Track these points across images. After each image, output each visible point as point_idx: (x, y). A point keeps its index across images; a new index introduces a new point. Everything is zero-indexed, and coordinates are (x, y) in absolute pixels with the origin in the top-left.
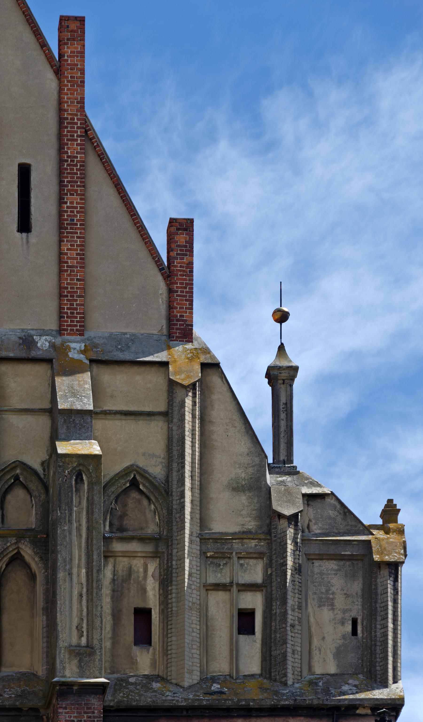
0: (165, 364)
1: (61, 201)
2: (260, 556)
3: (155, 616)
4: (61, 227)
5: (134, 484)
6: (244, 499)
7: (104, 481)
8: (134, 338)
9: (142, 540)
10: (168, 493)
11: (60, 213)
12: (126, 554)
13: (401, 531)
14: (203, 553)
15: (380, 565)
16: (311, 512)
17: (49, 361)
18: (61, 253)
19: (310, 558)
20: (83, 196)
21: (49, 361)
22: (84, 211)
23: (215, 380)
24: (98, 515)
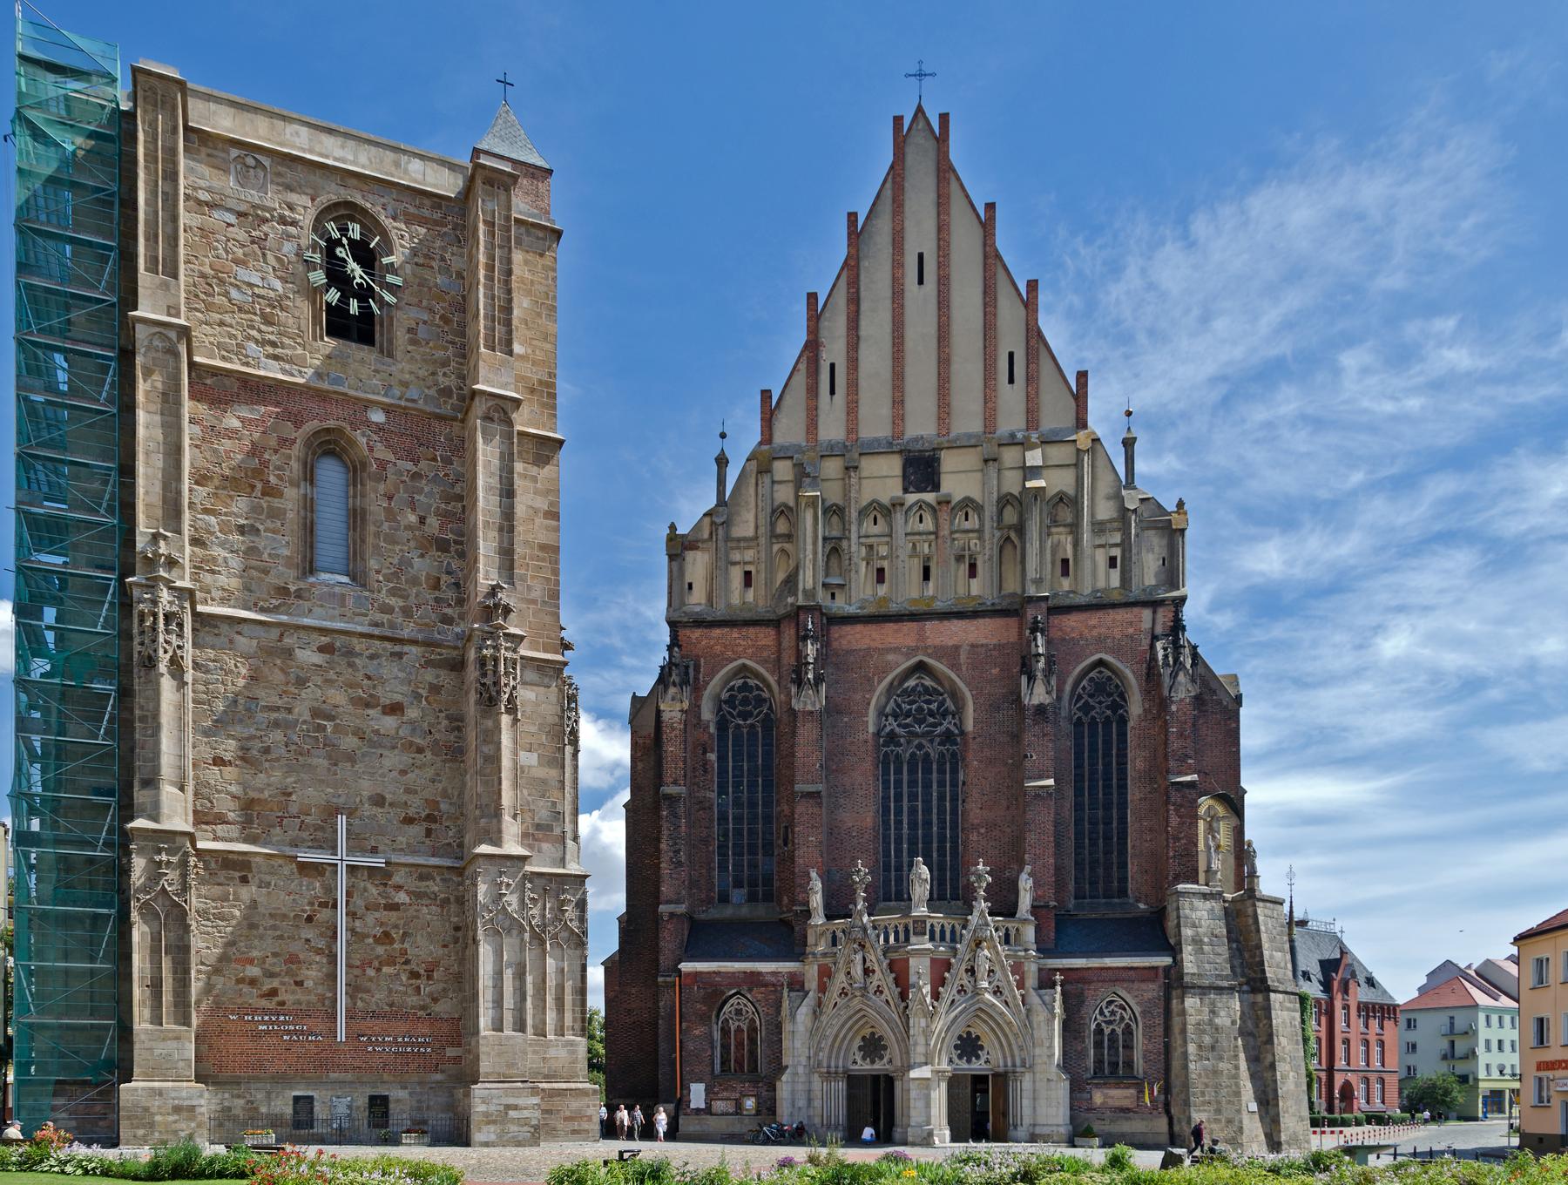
0: (1075, 441)
1: (1028, 367)
4: (1028, 380)
5: (1061, 499)
6: (1112, 503)
7: (1047, 498)
8: (1061, 429)
9: (1065, 526)
10: (1077, 502)
11: (1027, 373)
12: (1058, 533)
13: (1186, 513)
14: (1093, 531)
16: (1143, 507)
17: (1022, 444)
18: (1027, 392)
19: (1143, 529)
20: (1038, 364)
21: (1022, 444)
22: (1038, 371)
23: (1098, 446)
24: (1045, 515)
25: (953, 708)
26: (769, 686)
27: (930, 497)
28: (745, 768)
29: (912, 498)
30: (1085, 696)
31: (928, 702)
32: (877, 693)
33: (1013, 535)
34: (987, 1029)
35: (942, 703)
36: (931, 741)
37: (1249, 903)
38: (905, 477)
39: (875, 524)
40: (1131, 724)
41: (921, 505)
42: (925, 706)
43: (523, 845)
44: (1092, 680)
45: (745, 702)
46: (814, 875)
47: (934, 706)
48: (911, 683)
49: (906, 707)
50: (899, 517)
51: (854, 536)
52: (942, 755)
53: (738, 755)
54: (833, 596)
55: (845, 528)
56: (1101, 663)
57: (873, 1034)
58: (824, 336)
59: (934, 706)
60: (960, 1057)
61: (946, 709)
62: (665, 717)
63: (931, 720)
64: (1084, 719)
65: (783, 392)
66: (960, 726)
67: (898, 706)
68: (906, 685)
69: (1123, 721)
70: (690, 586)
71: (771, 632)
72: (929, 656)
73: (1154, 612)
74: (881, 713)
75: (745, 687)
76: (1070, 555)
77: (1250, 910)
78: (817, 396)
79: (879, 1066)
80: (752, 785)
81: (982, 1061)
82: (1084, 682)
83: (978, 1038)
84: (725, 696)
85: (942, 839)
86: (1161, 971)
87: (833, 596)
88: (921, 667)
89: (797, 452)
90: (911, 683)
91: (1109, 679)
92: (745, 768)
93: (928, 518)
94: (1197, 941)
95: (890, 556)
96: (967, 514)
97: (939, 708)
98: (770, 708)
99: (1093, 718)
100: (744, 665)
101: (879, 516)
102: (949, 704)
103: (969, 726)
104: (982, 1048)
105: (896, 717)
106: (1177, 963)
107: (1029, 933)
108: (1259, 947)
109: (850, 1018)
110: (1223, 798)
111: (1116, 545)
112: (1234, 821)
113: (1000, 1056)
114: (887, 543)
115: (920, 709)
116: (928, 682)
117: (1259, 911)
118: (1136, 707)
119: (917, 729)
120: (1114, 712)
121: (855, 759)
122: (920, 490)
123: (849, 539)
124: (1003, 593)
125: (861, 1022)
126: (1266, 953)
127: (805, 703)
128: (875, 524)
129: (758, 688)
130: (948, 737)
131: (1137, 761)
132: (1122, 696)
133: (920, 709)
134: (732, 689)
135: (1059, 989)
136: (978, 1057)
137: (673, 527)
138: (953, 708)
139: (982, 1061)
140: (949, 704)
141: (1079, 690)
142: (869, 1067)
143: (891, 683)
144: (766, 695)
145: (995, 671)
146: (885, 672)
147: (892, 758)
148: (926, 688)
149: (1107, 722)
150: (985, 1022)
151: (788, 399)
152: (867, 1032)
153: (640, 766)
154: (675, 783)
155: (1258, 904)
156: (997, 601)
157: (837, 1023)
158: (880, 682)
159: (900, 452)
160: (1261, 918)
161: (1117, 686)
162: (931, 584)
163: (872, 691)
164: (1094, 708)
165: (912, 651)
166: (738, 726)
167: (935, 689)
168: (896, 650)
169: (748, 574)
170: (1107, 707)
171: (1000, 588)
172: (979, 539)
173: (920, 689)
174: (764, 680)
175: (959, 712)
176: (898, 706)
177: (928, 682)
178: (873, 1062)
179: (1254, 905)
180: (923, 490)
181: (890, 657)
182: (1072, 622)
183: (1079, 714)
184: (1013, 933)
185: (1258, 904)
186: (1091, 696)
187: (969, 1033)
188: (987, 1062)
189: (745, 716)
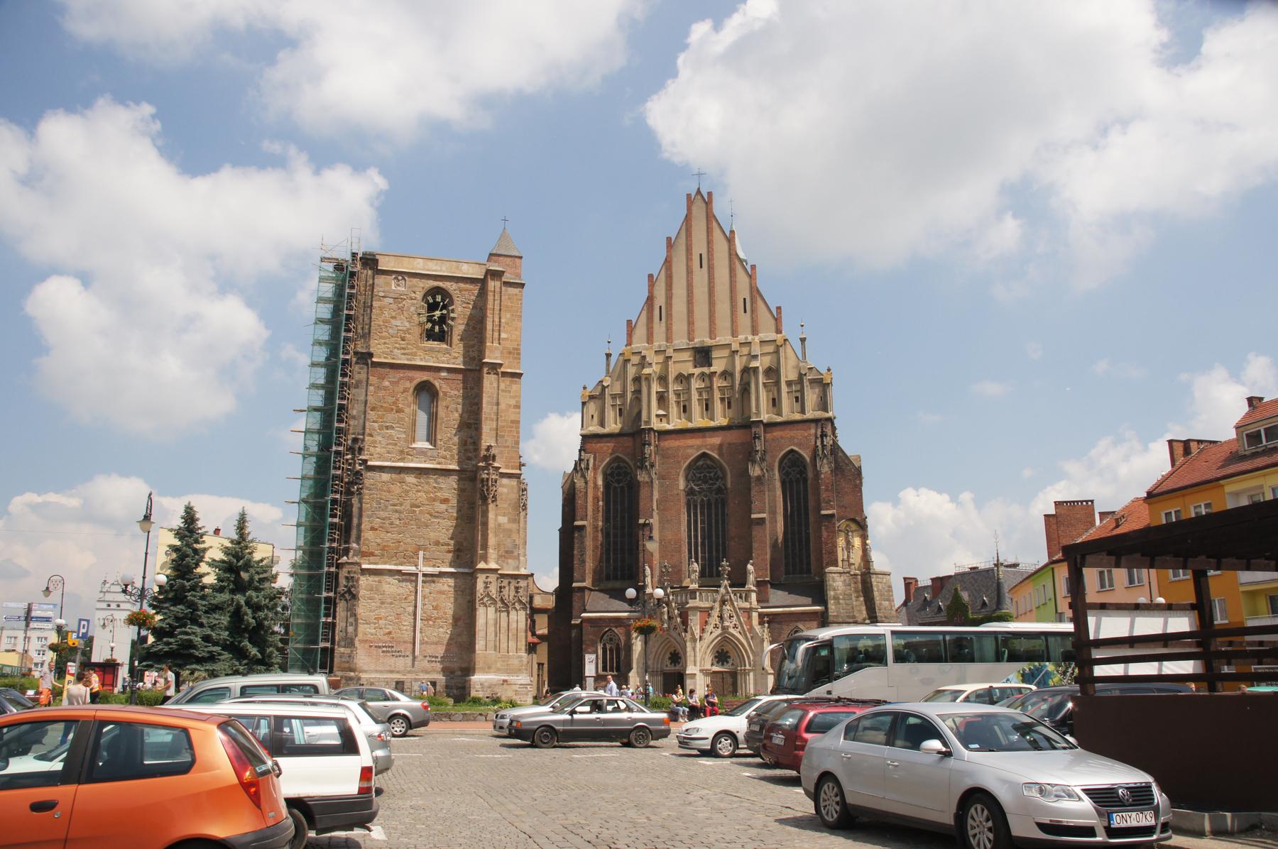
2: (799, 383)
3: (777, 400)
15: (825, 384)
25: (721, 475)
26: (630, 466)
27: (706, 370)
28: (619, 509)
29: (697, 371)
30: (787, 468)
31: (709, 472)
32: (683, 468)
33: (747, 386)
34: (731, 647)
35: (716, 474)
36: (711, 493)
37: (868, 576)
38: (695, 359)
39: (682, 383)
40: (809, 482)
41: (703, 374)
42: (708, 475)
43: (497, 564)
44: (789, 459)
45: (619, 474)
46: (647, 567)
47: (712, 475)
48: (701, 463)
49: (698, 475)
50: (693, 381)
51: (670, 390)
52: (717, 500)
53: (615, 502)
54: (661, 420)
55: (667, 387)
56: (792, 451)
57: (675, 651)
58: (656, 293)
59: (712, 475)
60: (718, 662)
61: (718, 476)
62: (578, 485)
63: (711, 482)
64: (787, 480)
65: (637, 321)
66: (724, 485)
67: (694, 475)
68: (698, 464)
69: (805, 480)
70: (592, 416)
71: (630, 439)
72: (708, 449)
73: (817, 425)
74: (687, 479)
75: (618, 467)
76: (776, 397)
77: (869, 580)
78: (652, 322)
79: (678, 667)
80: (623, 518)
81: (730, 664)
82: (786, 461)
83: (727, 652)
84: (608, 472)
85: (717, 545)
86: (819, 614)
87: (661, 420)
88: (704, 455)
89: (644, 350)
90: (701, 463)
91: (798, 458)
92: (619, 509)
93: (707, 380)
94: (836, 598)
95: (689, 399)
96: (725, 377)
97: (715, 476)
98: (631, 477)
99: (791, 479)
100: (618, 458)
101: (683, 379)
102: (719, 473)
103: (729, 485)
104: (729, 657)
105: (693, 481)
106: (827, 609)
107: (754, 596)
108: (873, 599)
109: (663, 642)
110: (853, 520)
111: (798, 391)
112: (861, 532)
113: (738, 661)
114: (687, 393)
115: (705, 476)
116: (709, 462)
117: (873, 580)
118: (810, 475)
119: (704, 486)
120: (801, 476)
121: (672, 503)
122: (702, 366)
123: (668, 391)
124: (744, 416)
125: (668, 645)
126: (877, 602)
127: (644, 477)
128: (682, 383)
129: (626, 468)
130: (719, 491)
131: (811, 504)
132: (805, 467)
133: (705, 476)
134: (612, 468)
135: (766, 625)
136: (727, 662)
137: (585, 388)
138: (721, 475)
139: (730, 664)
140: (719, 473)
141: (784, 464)
142: (673, 668)
143: (690, 463)
144: (629, 471)
145: (741, 457)
146: (687, 458)
147: (692, 502)
148: (708, 465)
149: (798, 481)
150: (730, 644)
151: (639, 322)
152: (672, 650)
153: (567, 509)
154: (582, 520)
155: (872, 576)
156: (740, 421)
157: (657, 646)
158: (685, 462)
159: (693, 348)
160: (874, 584)
161: (802, 462)
162: (709, 411)
163: (681, 468)
164: (791, 473)
165: (699, 448)
166: (615, 487)
167: (712, 466)
168: (691, 447)
169: (620, 410)
170: (798, 473)
171: (743, 414)
172: (731, 389)
173: (705, 466)
174: (627, 463)
175: (724, 478)
176: (694, 475)
177: (709, 462)
178: (675, 666)
179: (870, 577)
180: (704, 366)
181: (689, 451)
182: (777, 433)
183: (784, 477)
184: (744, 595)
185: (872, 576)
186: (789, 467)
187: (722, 650)
188: (733, 664)
189: (618, 482)
